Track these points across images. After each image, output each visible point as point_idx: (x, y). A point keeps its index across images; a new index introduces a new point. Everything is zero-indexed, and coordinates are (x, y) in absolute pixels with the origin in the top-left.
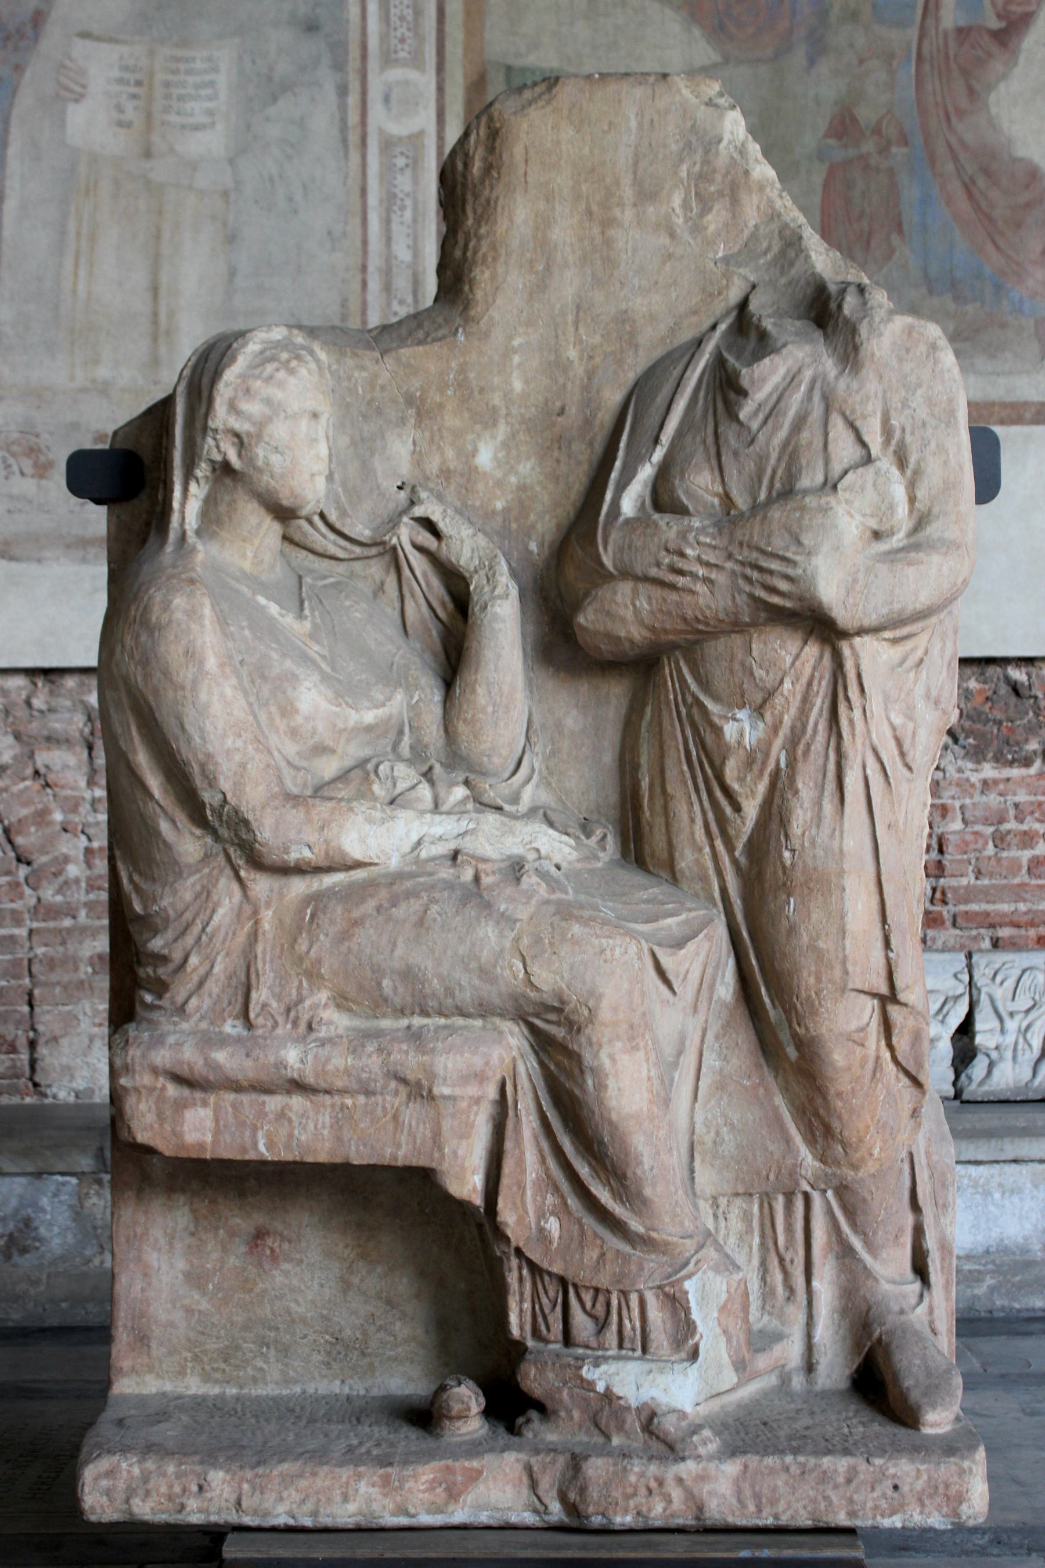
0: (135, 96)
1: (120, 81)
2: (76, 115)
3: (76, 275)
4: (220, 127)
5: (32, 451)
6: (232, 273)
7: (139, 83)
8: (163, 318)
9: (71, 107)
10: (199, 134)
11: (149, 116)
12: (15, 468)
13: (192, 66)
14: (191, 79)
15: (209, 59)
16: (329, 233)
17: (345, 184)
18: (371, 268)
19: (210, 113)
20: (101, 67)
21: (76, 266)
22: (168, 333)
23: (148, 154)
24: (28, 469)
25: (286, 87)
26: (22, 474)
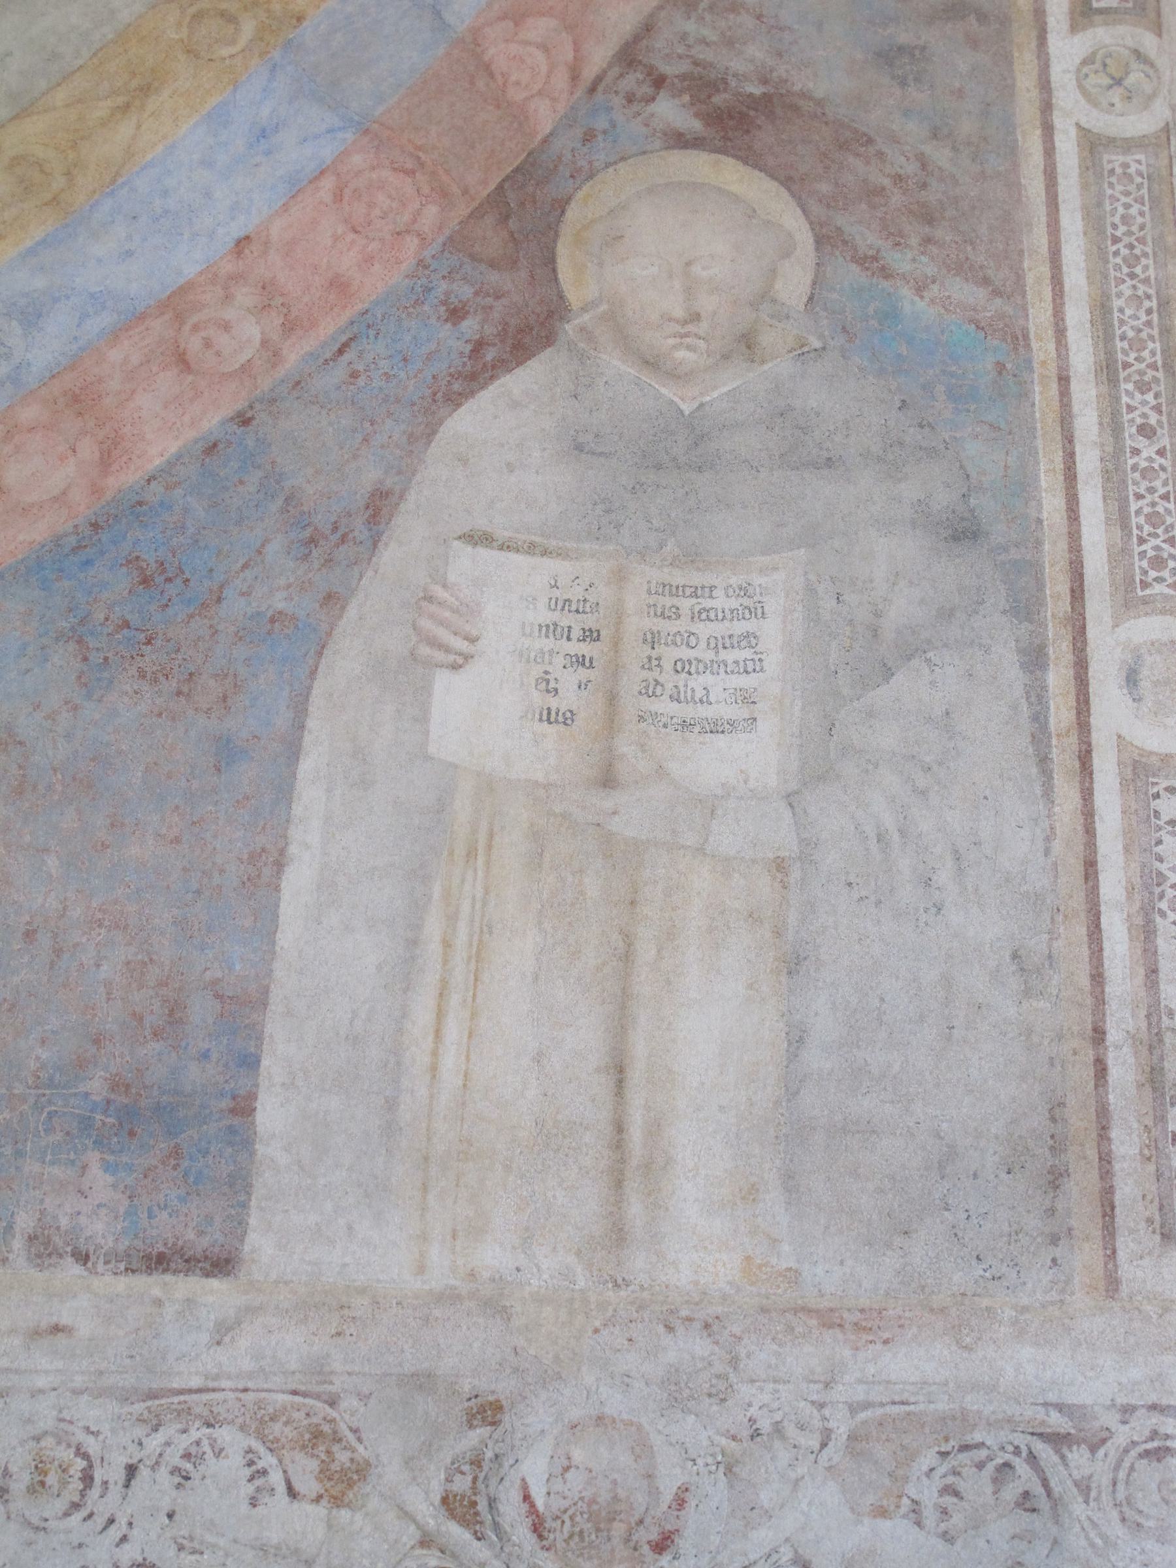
0: (581, 661)
1: (551, 630)
2: (451, 694)
3: (438, 1034)
4: (767, 726)
5: (318, 1438)
6: (797, 1039)
7: (591, 635)
8: (636, 1134)
9: (442, 680)
10: (721, 741)
11: (612, 699)
12: (276, 1478)
13: (708, 603)
14: (704, 630)
15: (744, 591)
16: (1015, 956)
17: (1047, 852)
18: (1114, 1035)
19: (747, 698)
20: (510, 600)
21: (440, 1014)
22: (647, 1167)
23: (607, 780)
24: (307, 1485)
25: (912, 648)
26: (292, 1493)
